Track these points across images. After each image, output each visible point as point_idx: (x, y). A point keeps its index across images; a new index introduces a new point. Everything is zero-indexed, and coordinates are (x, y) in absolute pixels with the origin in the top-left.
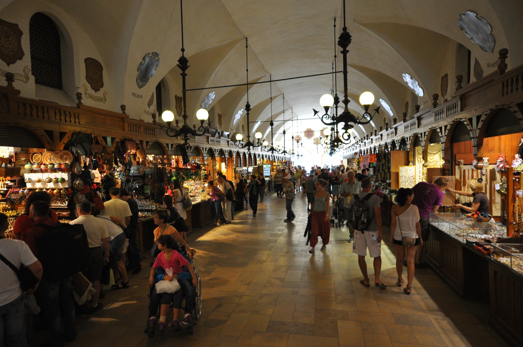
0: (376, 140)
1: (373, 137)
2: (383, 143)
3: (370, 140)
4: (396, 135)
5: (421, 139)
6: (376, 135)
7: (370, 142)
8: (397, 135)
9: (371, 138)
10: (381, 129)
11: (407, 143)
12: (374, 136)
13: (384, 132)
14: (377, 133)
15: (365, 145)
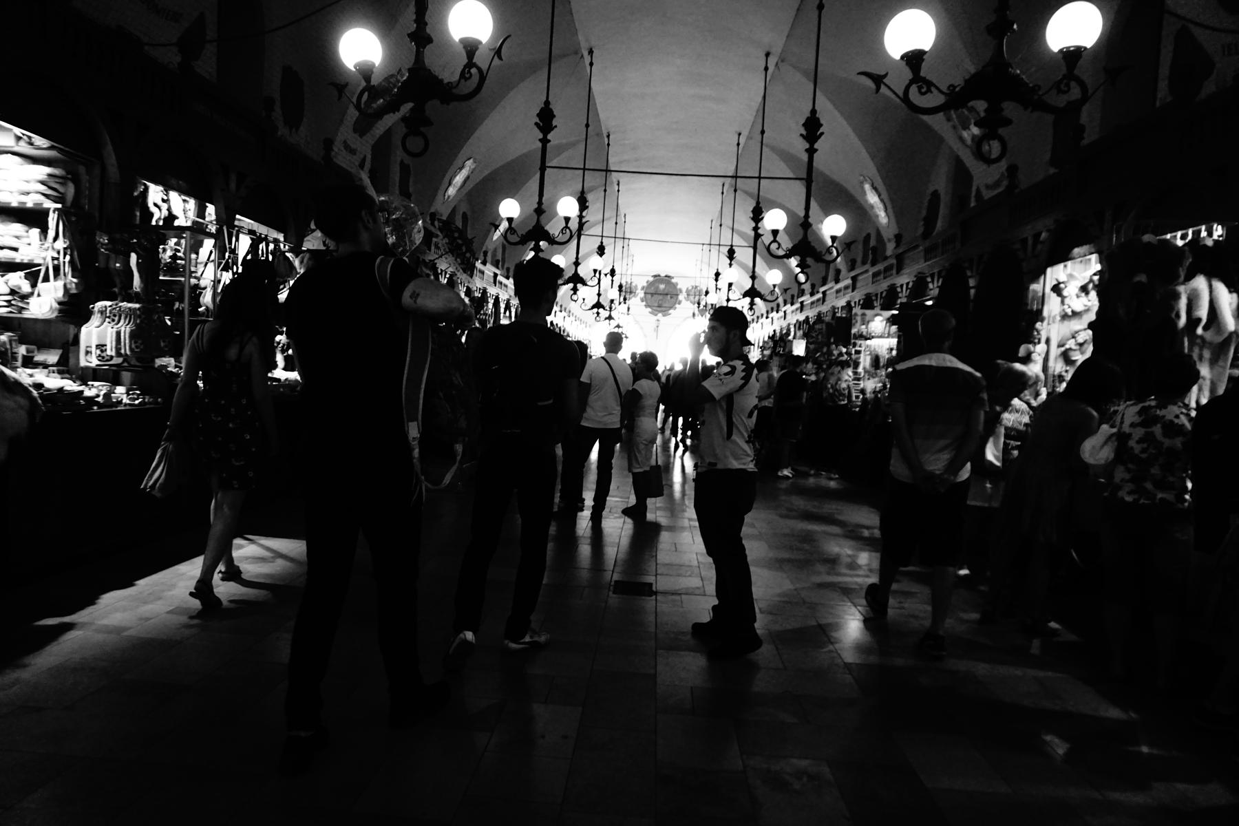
0: (812, 303)
1: (807, 299)
2: (824, 308)
3: (797, 305)
4: (823, 304)
5: (900, 295)
6: (812, 294)
7: (797, 309)
8: (825, 303)
9: (800, 300)
10: (824, 283)
11: (876, 305)
12: (809, 296)
13: (831, 287)
14: (815, 291)
15: (772, 324)
